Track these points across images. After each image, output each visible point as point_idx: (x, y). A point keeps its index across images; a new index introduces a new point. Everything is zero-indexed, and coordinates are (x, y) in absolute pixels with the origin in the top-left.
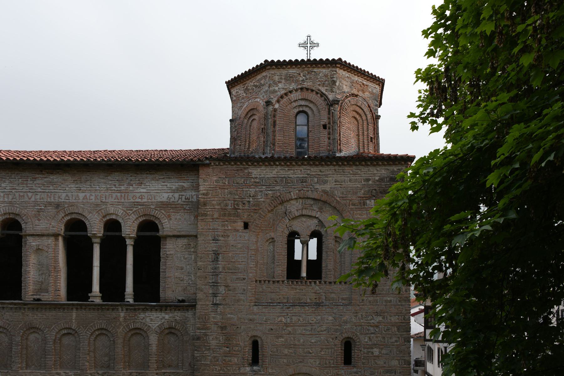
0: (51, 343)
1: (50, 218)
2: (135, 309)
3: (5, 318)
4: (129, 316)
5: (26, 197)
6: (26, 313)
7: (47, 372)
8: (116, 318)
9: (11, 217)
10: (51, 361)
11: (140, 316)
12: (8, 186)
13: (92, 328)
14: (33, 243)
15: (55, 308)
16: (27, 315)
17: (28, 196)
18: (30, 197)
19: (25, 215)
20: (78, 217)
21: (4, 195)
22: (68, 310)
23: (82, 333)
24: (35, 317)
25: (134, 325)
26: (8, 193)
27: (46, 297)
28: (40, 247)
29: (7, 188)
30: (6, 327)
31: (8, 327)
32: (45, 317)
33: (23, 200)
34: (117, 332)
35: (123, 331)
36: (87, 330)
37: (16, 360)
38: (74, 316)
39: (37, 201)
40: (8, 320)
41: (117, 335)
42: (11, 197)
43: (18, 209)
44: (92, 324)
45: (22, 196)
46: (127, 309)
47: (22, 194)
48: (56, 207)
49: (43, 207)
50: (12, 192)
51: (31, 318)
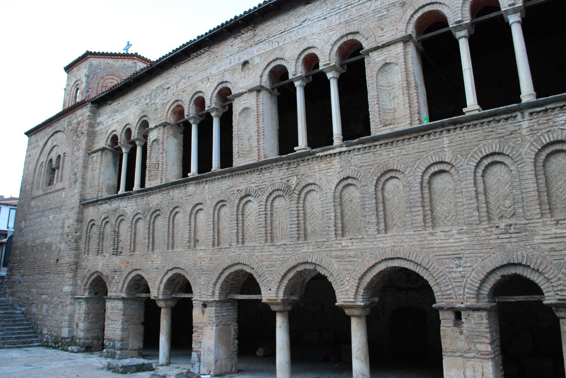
0: (417, 188)
1: (396, 22)
2: (546, 111)
3: (353, 164)
4: (539, 124)
5: (364, 8)
6: (378, 152)
7: (416, 233)
8: (516, 131)
9: (349, 39)
10: (419, 215)
11: (558, 119)
12: (343, 4)
13: (477, 155)
14: (378, 59)
15: (416, 137)
16: (380, 155)
17: (366, 7)
18: (368, 7)
19: (365, 29)
20: (431, 9)
21: (340, 16)
22: (435, 136)
23: (461, 166)
24: (391, 155)
25: (549, 137)
26: (344, 12)
27: (403, 124)
28: (388, 61)
29: (341, 7)
30: (355, 176)
31: (357, 176)
32: (404, 152)
33: (360, 14)
34: (520, 155)
35: (532, 150)
36: (470, 160)
37: (373, 219)
38: (447, 142)
39: (377, 9)
40: (356, 166)
41: (522, 159)
42: (347, 16)
43: (356, 26)
44: (476, 149)
45: (359, 9)
46: (531, 114)
47: (359, 7)
48: (403, 5)
49: (385, 13)
50: (347, 9)
51: (386, 157)
